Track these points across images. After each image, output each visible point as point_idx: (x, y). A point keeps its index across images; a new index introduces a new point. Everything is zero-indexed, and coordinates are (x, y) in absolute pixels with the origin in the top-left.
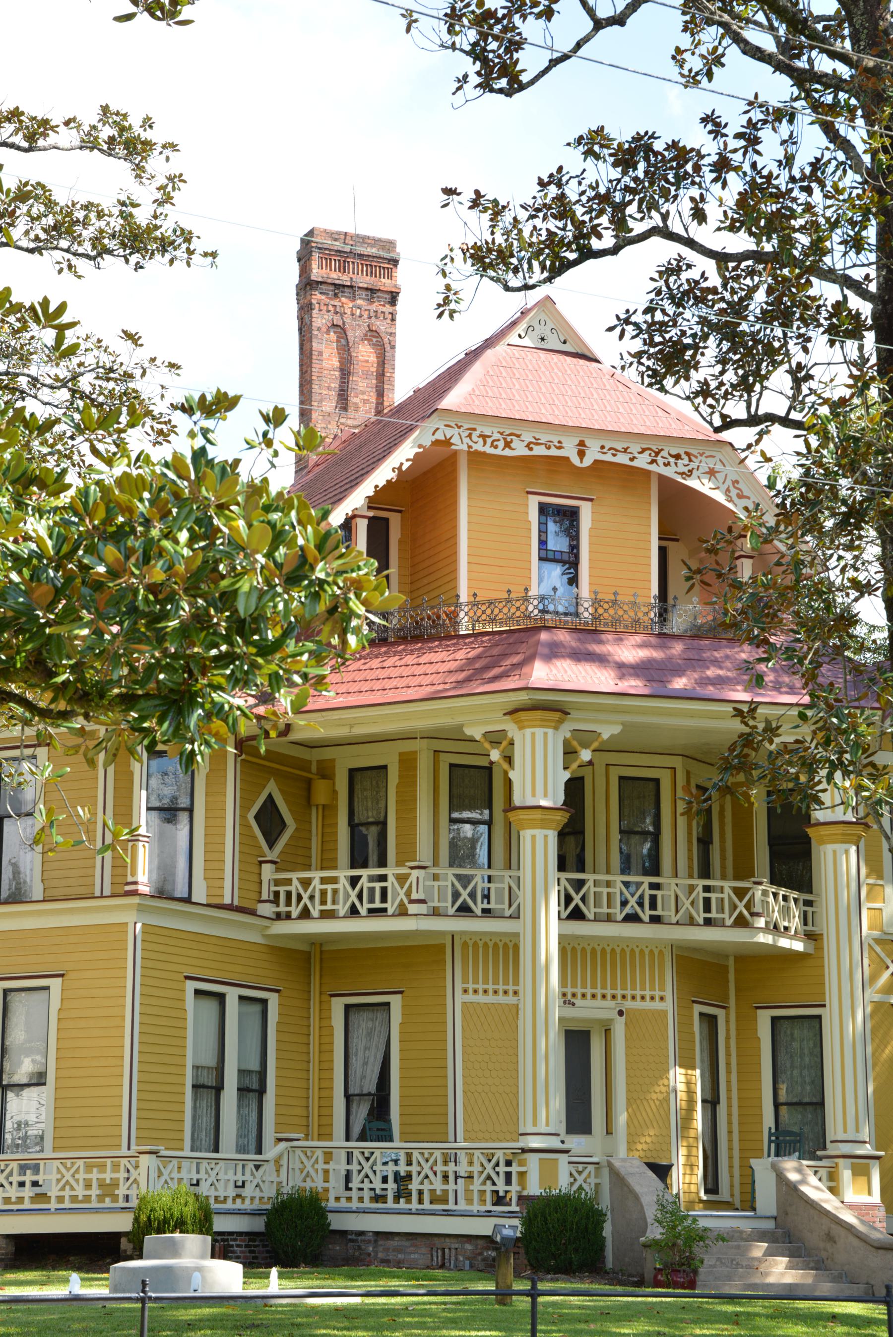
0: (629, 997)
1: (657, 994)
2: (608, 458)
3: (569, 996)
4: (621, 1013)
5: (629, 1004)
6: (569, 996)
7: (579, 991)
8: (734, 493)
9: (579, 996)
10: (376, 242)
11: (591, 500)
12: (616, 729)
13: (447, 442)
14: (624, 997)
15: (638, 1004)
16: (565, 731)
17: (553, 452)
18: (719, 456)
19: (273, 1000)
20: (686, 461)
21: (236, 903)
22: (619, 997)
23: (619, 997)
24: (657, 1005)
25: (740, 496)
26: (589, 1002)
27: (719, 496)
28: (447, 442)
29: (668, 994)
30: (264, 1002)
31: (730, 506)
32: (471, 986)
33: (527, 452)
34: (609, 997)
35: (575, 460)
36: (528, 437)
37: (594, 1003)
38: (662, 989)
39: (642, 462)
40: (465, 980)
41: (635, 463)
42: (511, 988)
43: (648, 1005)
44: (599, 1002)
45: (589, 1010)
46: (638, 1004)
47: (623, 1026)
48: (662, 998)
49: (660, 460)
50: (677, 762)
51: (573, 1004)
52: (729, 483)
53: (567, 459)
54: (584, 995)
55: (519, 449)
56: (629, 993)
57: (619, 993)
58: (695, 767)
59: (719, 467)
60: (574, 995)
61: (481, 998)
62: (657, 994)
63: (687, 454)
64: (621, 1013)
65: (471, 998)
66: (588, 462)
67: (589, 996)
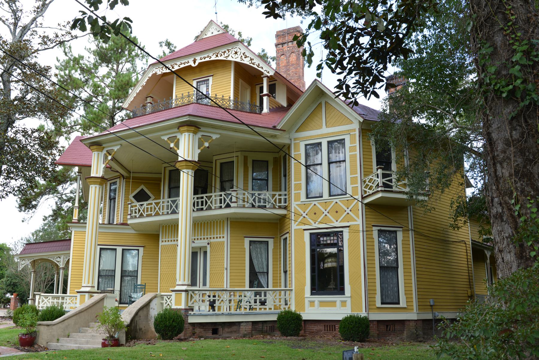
1: (221, 236)
2: (203, 60)
4: (208, 244)
5: (212, 240)
8: (243, 56)
10: (293, 28)
11: (212, 76)
12: (118, 147)
13: (156, 73)
15: (215, 240)
16: (104, 152)
17: (187, 65)
18: (238, 47)
19: (141, 249)
20: (227, 52)
21: (122, 222)
24: (222, 240)
25: (245, 57)
26: (199, 241)
27: (238, 60)
28: (156, 73)
29: (225, 236)
30: (138, 250)
31: (242, 62)
32: (164, 240)
33: (179, 68)
35: (193, 65)
36: (178, 63)
38: (223, 234)
39: (214, 58)
40: (162, 238)
41: (211, 59)
42: (176, 239)
43: (219, 240)
44: (202, 241)
45: (199, 243)
48: (223, 237)
49: (219, 55)
50: (239, 154)
52: (242, 54)
53: (191, 65)
54: (198, 239)
55: (176, 68)
58: (246, 154)
59: (238, 50)
60: (195, 239)
61: (167, 243)
62: (221, 236)
63: (228, 50)
64: (208, 244)
65: (164, 243)
66: (197, 64)
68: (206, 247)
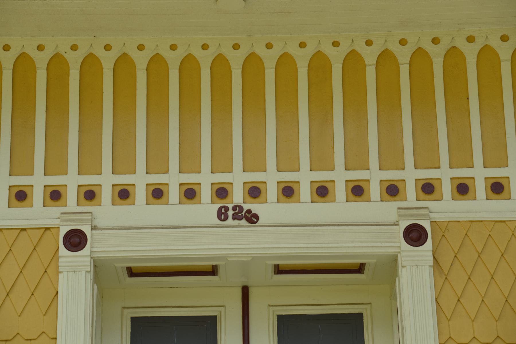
0: (447, 189)
3: (238, 196)
4: (415, 235)
5: (446, 208)
6: (238, 196)
7: (271, 179)
9: (272, 192)
14: (428, 189)
22: (411, 190)
23: (411, 190)
26: (304, 208)
34: (375, 191)
37: (323, 210)
46: (481, 207)
47: (426, 274)
51: (252, 218)
54: (288, 192)
56: (445, 175)
57: (410, 176)
60: (255, 192)
64: (415, 235)
67: (305, 191)
68: (391, 265)
